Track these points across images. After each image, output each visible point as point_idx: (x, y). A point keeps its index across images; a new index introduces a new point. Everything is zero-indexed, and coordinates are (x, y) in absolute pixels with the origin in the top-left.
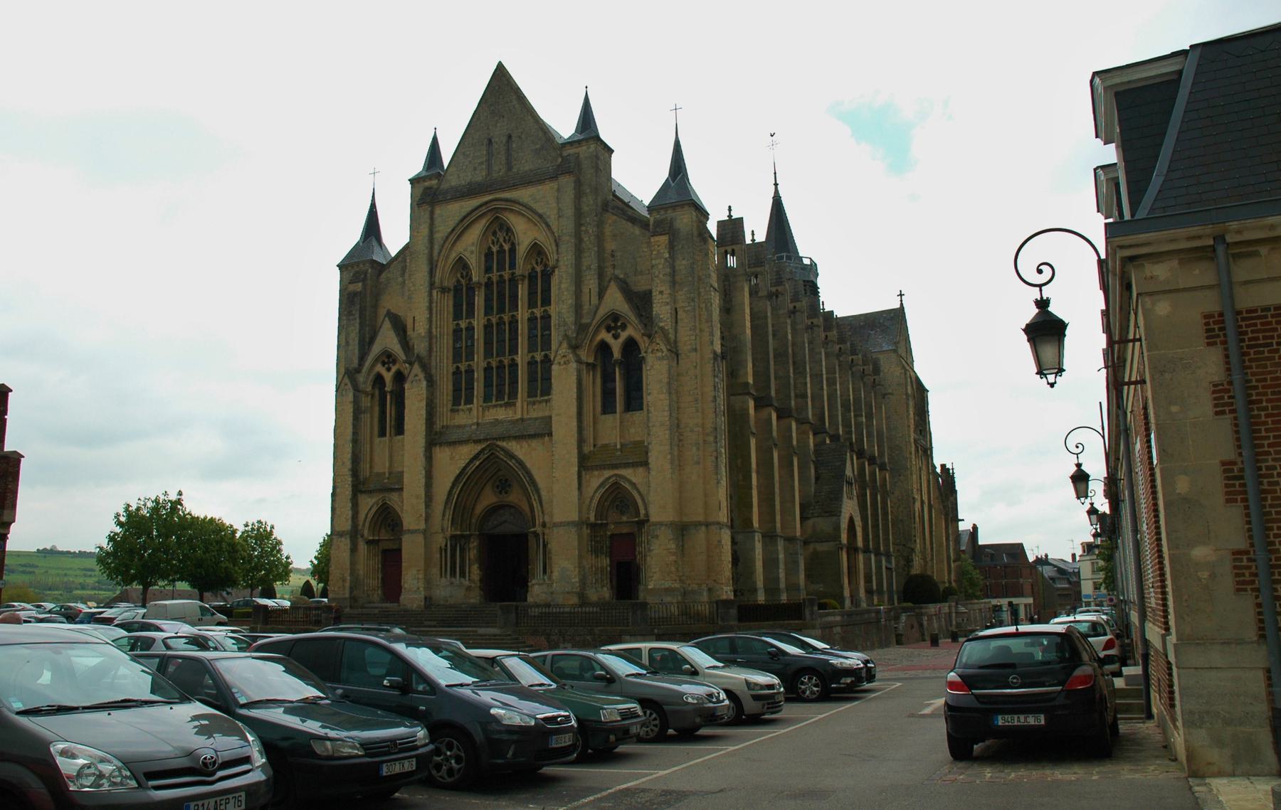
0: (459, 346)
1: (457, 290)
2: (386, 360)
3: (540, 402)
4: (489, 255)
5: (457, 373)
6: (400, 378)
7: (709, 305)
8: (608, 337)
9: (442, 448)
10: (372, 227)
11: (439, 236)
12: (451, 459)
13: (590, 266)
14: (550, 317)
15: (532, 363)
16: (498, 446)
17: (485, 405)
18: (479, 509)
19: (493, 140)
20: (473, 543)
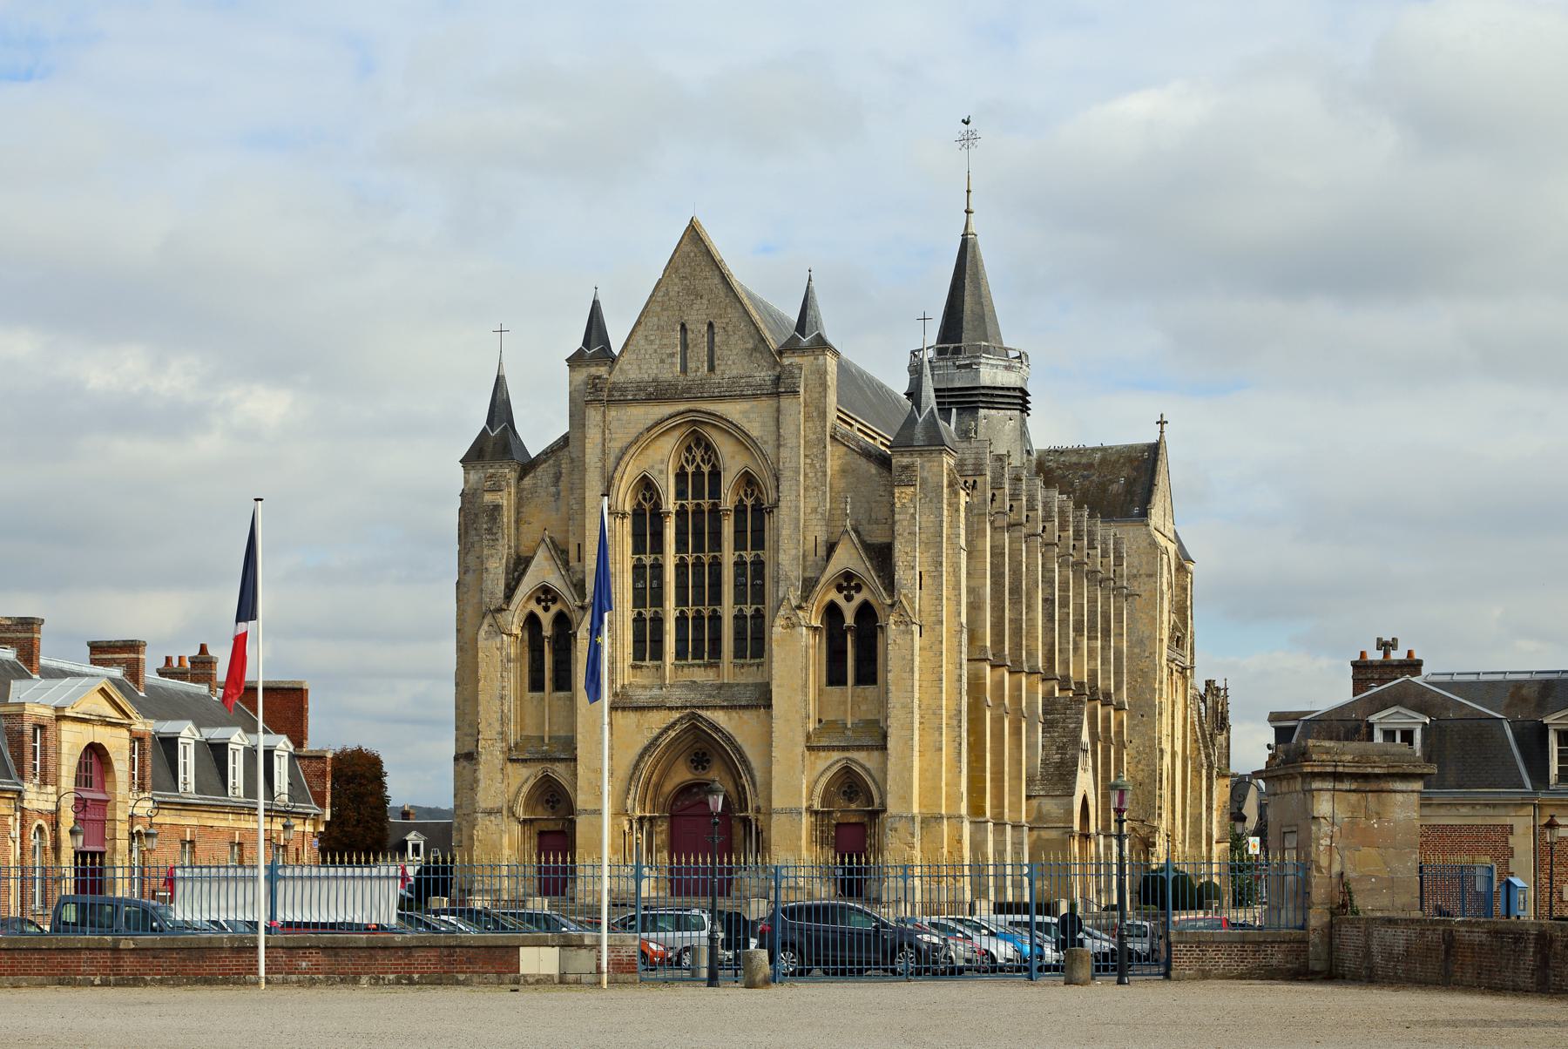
0: (640, 586)
1: (638, 514)
2: (543, 597)
3: (751, 665)
4: (681, 476)
5: (639, 621)
6: (562, 621)
7: (957, 569)
8: (840, 599)
9: (625, 713)
10: (500, 410)
11: (615, 446)
12: (637, 726)
13: (817, 508)
14: (762, 563)
15: (739, 618)
16: (700, 716)
17: (677, 662)
18: (670, 786)
19: (688, 326)
20: (660, 826)
